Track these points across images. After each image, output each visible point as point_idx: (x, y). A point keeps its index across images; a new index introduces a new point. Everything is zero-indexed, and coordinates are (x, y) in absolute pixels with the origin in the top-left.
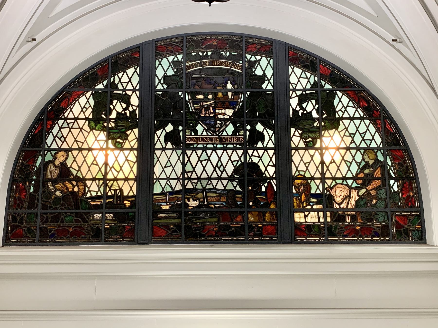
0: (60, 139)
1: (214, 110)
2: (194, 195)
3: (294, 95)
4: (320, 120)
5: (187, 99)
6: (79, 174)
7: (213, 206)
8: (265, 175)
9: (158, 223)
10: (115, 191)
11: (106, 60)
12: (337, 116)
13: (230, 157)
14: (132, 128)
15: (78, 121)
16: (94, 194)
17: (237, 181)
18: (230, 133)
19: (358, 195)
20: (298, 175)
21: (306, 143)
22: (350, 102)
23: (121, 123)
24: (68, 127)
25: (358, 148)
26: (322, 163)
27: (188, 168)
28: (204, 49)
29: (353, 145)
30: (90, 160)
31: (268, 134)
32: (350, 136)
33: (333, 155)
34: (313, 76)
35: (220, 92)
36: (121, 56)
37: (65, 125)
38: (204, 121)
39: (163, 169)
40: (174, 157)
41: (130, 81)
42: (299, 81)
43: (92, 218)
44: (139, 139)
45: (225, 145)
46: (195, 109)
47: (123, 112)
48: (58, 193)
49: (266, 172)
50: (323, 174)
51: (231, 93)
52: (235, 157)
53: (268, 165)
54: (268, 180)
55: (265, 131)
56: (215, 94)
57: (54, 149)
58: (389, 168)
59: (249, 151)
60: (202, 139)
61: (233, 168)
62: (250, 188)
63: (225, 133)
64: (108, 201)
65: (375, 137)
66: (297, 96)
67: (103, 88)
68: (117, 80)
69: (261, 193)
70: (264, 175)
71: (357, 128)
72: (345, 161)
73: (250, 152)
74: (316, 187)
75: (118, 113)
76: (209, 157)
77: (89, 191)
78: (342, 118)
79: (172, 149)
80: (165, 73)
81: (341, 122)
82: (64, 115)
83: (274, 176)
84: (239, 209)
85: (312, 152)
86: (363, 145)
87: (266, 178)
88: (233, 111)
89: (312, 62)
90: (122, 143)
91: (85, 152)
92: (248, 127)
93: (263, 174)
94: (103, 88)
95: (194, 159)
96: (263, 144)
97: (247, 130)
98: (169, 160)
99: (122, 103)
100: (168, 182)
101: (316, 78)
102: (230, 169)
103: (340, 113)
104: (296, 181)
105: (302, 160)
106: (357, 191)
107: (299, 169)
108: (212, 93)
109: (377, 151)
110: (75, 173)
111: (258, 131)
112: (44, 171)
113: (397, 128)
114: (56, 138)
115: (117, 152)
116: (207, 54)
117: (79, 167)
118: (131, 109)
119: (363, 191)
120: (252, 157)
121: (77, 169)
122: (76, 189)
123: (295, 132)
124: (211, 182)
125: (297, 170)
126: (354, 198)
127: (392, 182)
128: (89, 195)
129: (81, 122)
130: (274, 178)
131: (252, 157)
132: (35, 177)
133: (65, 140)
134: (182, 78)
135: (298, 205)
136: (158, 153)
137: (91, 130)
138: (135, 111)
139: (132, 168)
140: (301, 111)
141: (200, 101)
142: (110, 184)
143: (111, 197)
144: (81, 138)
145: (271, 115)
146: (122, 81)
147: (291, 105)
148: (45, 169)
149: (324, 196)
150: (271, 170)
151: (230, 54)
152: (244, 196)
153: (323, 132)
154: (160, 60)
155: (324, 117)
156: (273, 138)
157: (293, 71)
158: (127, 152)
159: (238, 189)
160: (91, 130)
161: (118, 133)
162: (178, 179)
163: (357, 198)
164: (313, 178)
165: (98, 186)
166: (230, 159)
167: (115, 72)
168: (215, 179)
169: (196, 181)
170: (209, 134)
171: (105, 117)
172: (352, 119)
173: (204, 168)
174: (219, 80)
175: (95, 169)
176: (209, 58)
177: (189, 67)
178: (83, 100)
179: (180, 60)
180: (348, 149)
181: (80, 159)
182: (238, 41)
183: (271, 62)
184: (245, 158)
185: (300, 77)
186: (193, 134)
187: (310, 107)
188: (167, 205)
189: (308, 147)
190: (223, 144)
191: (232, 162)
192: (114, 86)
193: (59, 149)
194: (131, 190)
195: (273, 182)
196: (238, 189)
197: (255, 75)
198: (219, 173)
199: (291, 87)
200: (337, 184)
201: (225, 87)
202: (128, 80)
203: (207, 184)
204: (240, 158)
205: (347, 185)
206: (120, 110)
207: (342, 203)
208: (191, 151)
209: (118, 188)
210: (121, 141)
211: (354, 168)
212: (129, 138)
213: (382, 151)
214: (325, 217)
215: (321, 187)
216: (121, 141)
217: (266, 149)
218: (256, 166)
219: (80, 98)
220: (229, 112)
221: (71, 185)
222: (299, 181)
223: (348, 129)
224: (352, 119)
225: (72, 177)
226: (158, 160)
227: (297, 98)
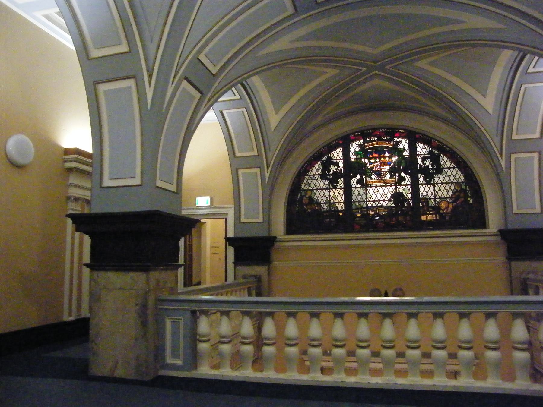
18: (388, 178)
25: (452, 183)
26: (435, 191)
27: (369, 196)
29: (450, 181)
30: (322, 194)
31: (407, 177)
44: (344, 183)
48: (309, 210)
50: (435, 196)
52: (391, 190)
60: (375, 182)
73: (399, 187)
74: (432, 203)
78: (444, 168)
85: (429, 186)
86: (455, 181)
95: (371, 191)
102: (389, 196)
110: (316, 200)
113: (472, 172)
115: (334, 190)
118: (339, 169)
122: (317, 208)
127: (469, 199)
129: (317, 177)
136: (353, 189)
148: (302, 199)
150: (409, 196)
158: (339, 190)
159: (393, 205)
162: (364, 202)
164: (430, 199)
177: (366, 146)
178: (317, 166)
180: (447, 183)
181: (317, 194)
184: (396, 190)
192: (330, 158)
193: (308, 190)
196: (393, 205)
206: (334, 169)
211: (450, 193)
214: (436, 217)
217: (406, 185)
218: (402, 194)
220: (387, 168)
224: (449, 168)
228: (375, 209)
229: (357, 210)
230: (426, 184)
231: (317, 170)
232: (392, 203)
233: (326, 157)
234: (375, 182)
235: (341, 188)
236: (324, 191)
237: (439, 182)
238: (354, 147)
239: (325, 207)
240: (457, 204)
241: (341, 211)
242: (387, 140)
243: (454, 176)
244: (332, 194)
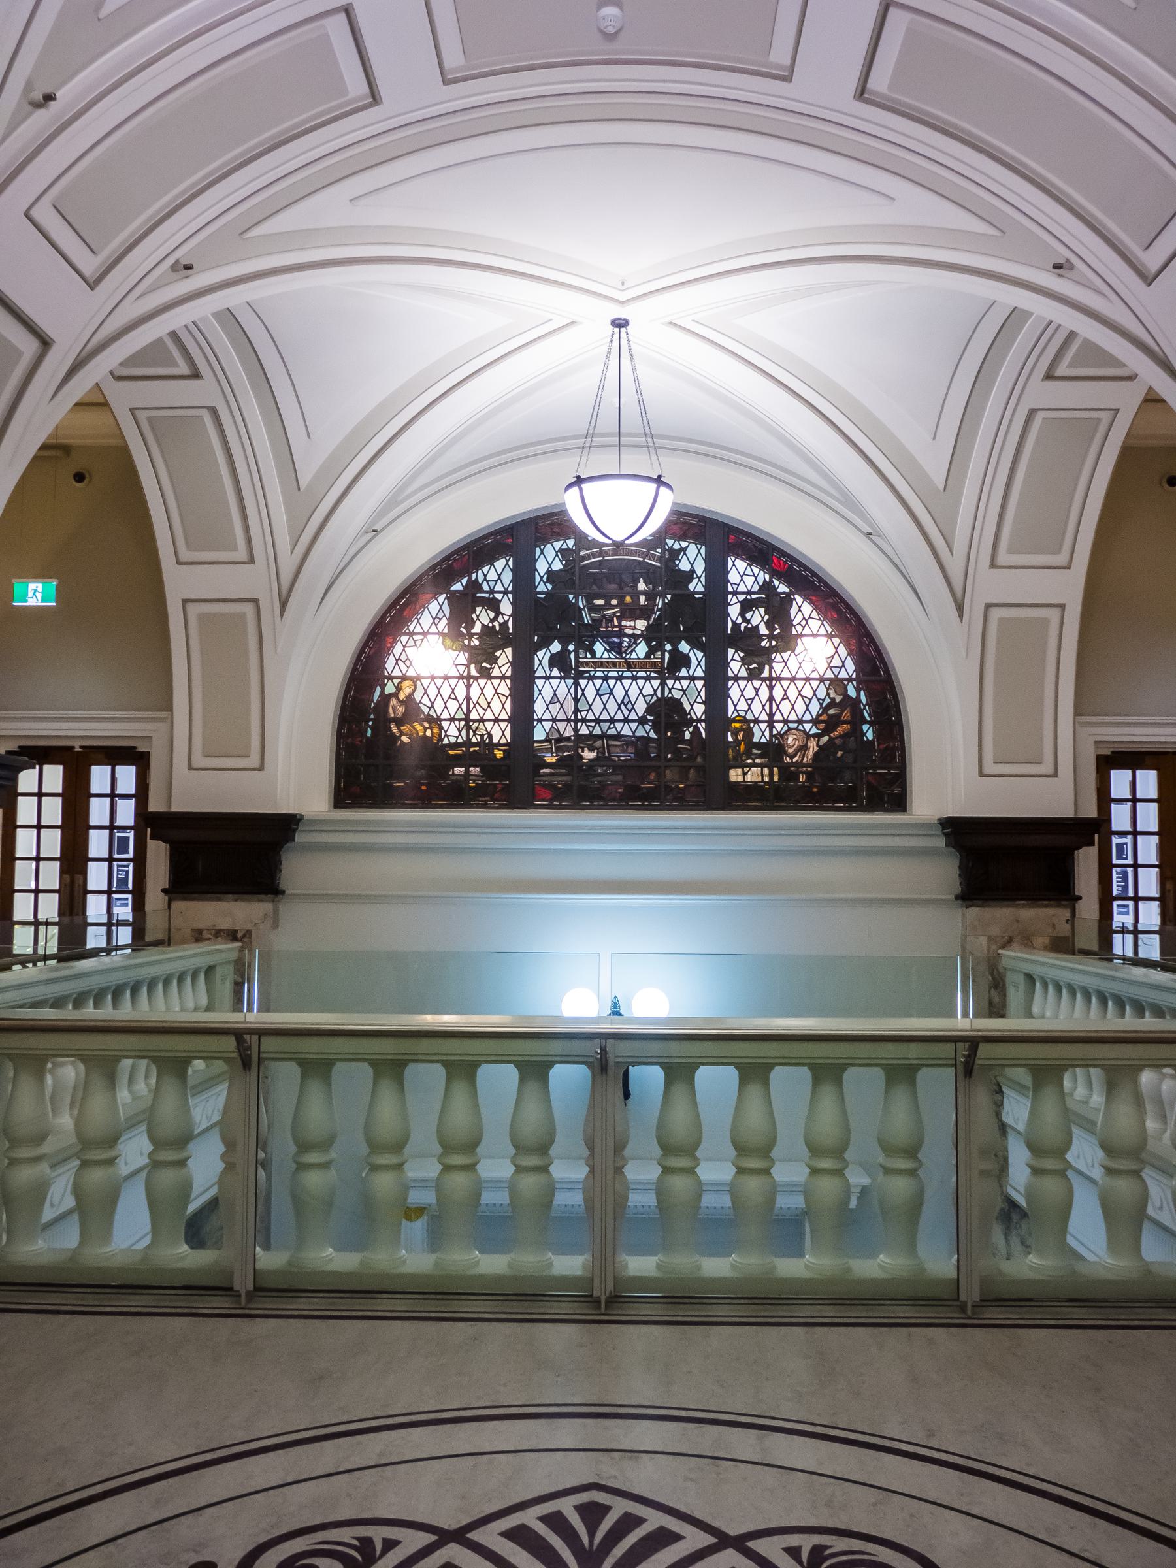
1: (620, 623)
3: (735, 600)
6: (432, 713)
10: (482, 736)
12: (794, 632)
14: (503, 647)
16: (453, 740)
18: (642, 656)
23: (488, 641)
26: (771, 699)
27: (582, 705)
31: (697, 657)
37: (411, 642)
38: (606, 637)
40: (564, 688)
44: (513, 664)
48: (405, 739)
50: (771, 715)
52: (648, 690)
56: (621, 599)
57: (396, 677)
60: (602, 664)
63: (634, 656)
69: (684, 742)
73: (670, 683)
74: (760, 734)
78: (800, 636)
79: (560, 678)
84: (653, 763)
85: (757, 683)
86: (829, 674)
87: (692, 720)
92: (668, 647)
95: (590, 692)
101: (767, 577)
102: (641, 707)
110: (426, 710)
113: (878, 650)
115: (482, 682)
117: (432, 703)
118: (500, 619)
119: (825, 739)
122: (428, 733)
128: (446, 741)
134: (573, 573)
135: (735, 758)
136: (539, 683)
140: (744, 625)
150: (699, 710)
152: (659, 745)
156: (703, 663)
158: (496, 682)
159: (652, 735)
162: (568, 721)
163: (816, 749)
164: (756, 721)
167: (478, 566)
169: (593, 724)
174: (626, 577)
175: (453, 706)
177: (584, 558)
178: (434, 607)
181: (432, 692)
183: (703, 551)
186: (589, 656)
189: (753, 675)
192: (475, 586)
193: (404, 678)
195: (702, 726)
196: (652, 735)
199: (730, 589)
200: (790, 729)
202: (496, 577)
204: (655, 691)
205: (804, 731)
207: (795, 755)
211: (815, 708)
214: (771, 774)
215: (767, 734)
217: (692, 679)
218: (677, 704)
220: (641, 625)
222: (737, 725)
228: (598, 744)
229: (545, 745)
230: (749, 679)
231: (435, 620)
232: (648, 727)
233: (464, 581)
235: (503, 678)
237: (786, 674)
238: (548, 559)
239: (452, 730)
241: (499, 744)
244: (475, 692)
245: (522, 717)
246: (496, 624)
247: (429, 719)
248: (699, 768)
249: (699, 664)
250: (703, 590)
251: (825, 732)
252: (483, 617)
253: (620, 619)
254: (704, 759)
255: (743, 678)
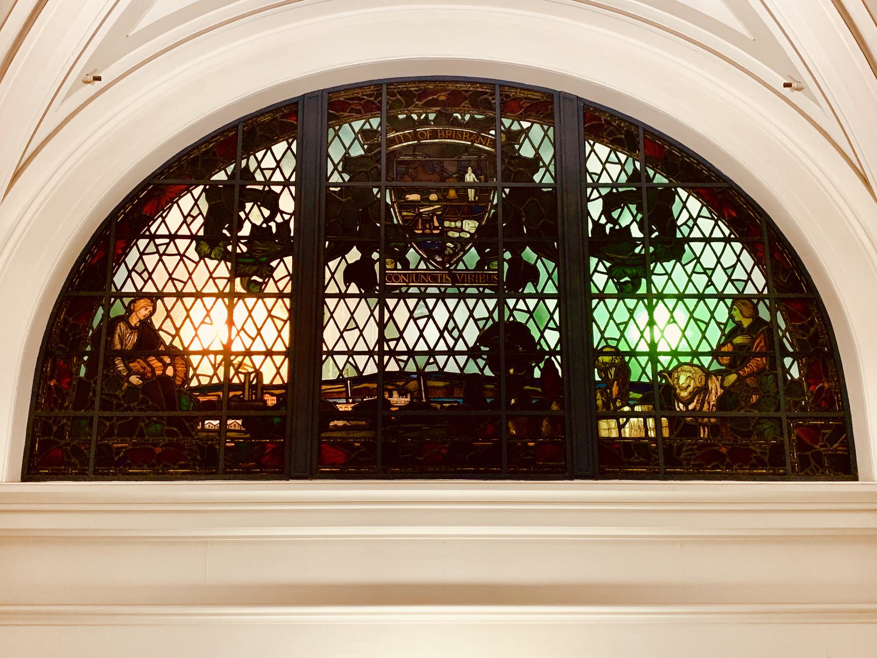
0: (140, 275)
2: (402, 383)
3: (595, 194)
4: (647, 242)
5: (388, 201)
6: (177, 343)
7: (439, 406)
8: (541, 346)
9: (331, 438)
11: (233, 127)
12: (679, 235)
13: (471, 312)
15: (177, 241)
16: (205, 381)
17: (485, 357)
18: (472, 265)
19: (722, 387)
20: (604, 347)
21: (619, 286)
22: (704, 208)
23: (260, 247)
24: (158, 252)
25: (721, 297)
27: (390, 332)
28: (422, 107)
29: (711, 290)
31: (545, 268)
32: (705, 273)
33: (669, 324)
34: (630, 159)
35: (453, 188)
36: (262, 119)
39: (342, 333)
41: (278, 166)
42: (604, 168)
43: (199, 427)
44: (294, 277)
45: (462, 289)
46: (403, 221)
47: (264, 225)
48: (134, 380)
49: (542, 341)
51: (473, 190)
52: (481, 312)
53: (546, 327)
54: (547, 357)
55: (539, 263)
56: (442, 192)
57: (128, 295)
58: (781, 334)
59: (508, 301)
60: (418, 277)
61: (477, 333)
62: (511, 371)
63: (461, 266)
64: (231, 394)
65: (752, 276)
66: (601, 196)
67: (226, 178)
68: (253, 165)
70: (538, 347)
71: (719, 259)
72: (696, 320)
73: (511, 302)
74: (639, 371)
75: (254, 226)
76: (431, 312)
77: (195, 375)
78: (688, 240)
79: (360, 296)
80: (347, 152)
81: (686, 246)
82: (148, 230)
83: (558, 349)
85: (631, 303)
86: (730, 290)
88: (477, 224)
89: (628, 133)
90: (261, 284)
91: (188, 301)
92: (508, 255)
93: (536, 344)
94: (226, 178)
95: (401, 315)
96: (535, 287)
97: (505, 260)
98: (352, 317)
99: (262, 208)
100: (351, 360)
101: (638, 164)
102: (472, 335)
103: (685, 230)
104: (600, 358)
105: (611, 318)
106: (720, 378)
107: (606, 335)
108: (437, 191)
109: (758, 303)
110: (167, 339)
111: (527, 264)
112: (108, 335)
114: (134, 274)
115: (250, 301)
116: (427, 118)
117: (178, 330)
118: (279, 219)
119: (733, 378)
120: (515, 313)
121: (173, 332)
122: (170, 371)
123: (597, 265)
124: (435, 359)
125: (602, 337)
126: (713, 391)
127: (788, 361)
128: (194, 383)
129: (182, 244)
130: (559, 353)
131: (515, 313)
132: (89, 348)
133: (150, 277)
134: (379, 161)
135: (606, 405)
136: (331, 302)
137: (202, 257)
138: (287, 223)
139: (279, 332)
140: (609, 226)
141: (414, 205)
142: (236, 362)
143: (240, 387)
144: (181, 274)
145: (552, 232)
146: (263, 166)
147: (589, 214)
148: (111, 332)
149: (656, 388)
150: (552, 338)
151: (472, 118)
152: (498, 387)
153: (652, 265)
154: (337, 128)
155: (653, 236)
157: (593, 150)
158: (270, 302)
159: (488, 372)
160: (202, 257)
161: (253, 264)
162: (370, 353)
163: (720, 391)
164: (633, 353)
165: (213, 366)
166: (471, 315)
168: (442, 353)
169: (405, 358)
170: (431, 267)
171: (228, 235)
172: (708, 240)
173: (421, 331)
174: (451, 167)
176: (430, 125)
177: (392, 141)
178: (186, 202)
179: (375, 127)
180: (701, 297)
181: (178, 314)
182: (486, 93)
183: (551, 132)
185: (607, 161)
186: (399, 266)
187: (626, 219)
188: (348, 403)
190: (458, 288)
191: (476, 321)
192: (247, 175)
193: (139, 295)
194: (278, 373)
195: (557, 360)
196: (488, 372)
197: (520, 156)
198: (451, 342)
199: (589, 180)
200: (681, 364)
201: (462, 178)
202: (274, 165)
203: (428, 363)
204: (491, 313)
205: (701, 367)
206: (258, 221)
207: (691, 401)
208: (396, 300)
209: (251, 370)
210: (260, 280)
211: (714, 335)
212: (274, 275)
213: (767, 301)
214: (658, 427)
216: (260, 280)
217: (542, 297)
218: (523, 329)
219: (180, 197)
220: (470, 226)
221: (161, 364)
222: (607, 359)
223: (701, 260)
224: (708, 240)
225: (162, 348)
226: (332, 317)
227: (601, 200)
229: (339, 388)
230: (620, 296)
231: (186, 219)
233: (230, 169)
234: (418, 277)
236: (209, 301)
237: (670, 290)
240: (740, 379)
241: (271, 387)
242: (473, 123)
243: (729, 272)
245: (306, 345)
246: (272, 224)
247: (172, 352)
248: (555, 420)
249: (550, 277)
250: (551, 181)
251: (731, 367)
252: (256, 215)
253: (441, 220)
254: (562, 407)
255: (611, 296)
